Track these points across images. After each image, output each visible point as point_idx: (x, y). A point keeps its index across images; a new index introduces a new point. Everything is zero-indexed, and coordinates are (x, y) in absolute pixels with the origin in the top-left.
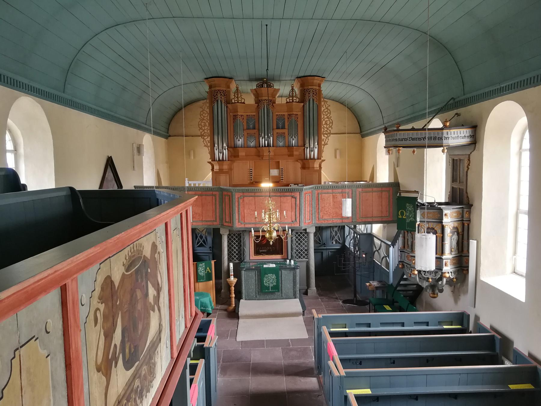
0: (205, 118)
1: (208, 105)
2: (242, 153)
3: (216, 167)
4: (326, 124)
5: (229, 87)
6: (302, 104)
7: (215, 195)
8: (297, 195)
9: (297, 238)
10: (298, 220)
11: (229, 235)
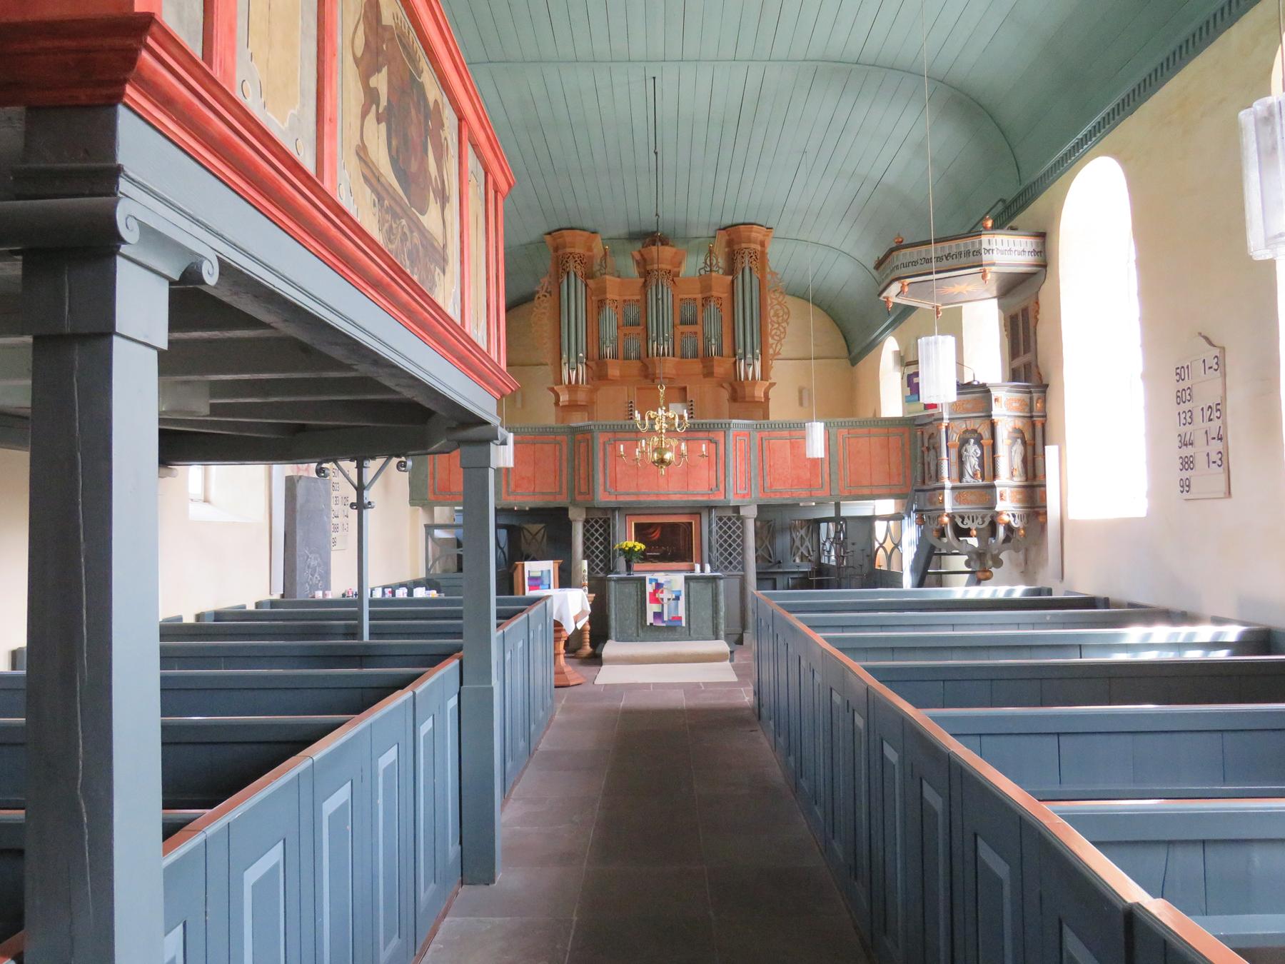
2: (614, 371)
3: (564, 398)
4: (776, 315)
5: (590, 249)
8: (720, 436)
9: (721, 528)
10: (721, 487)
11: (587, 521)
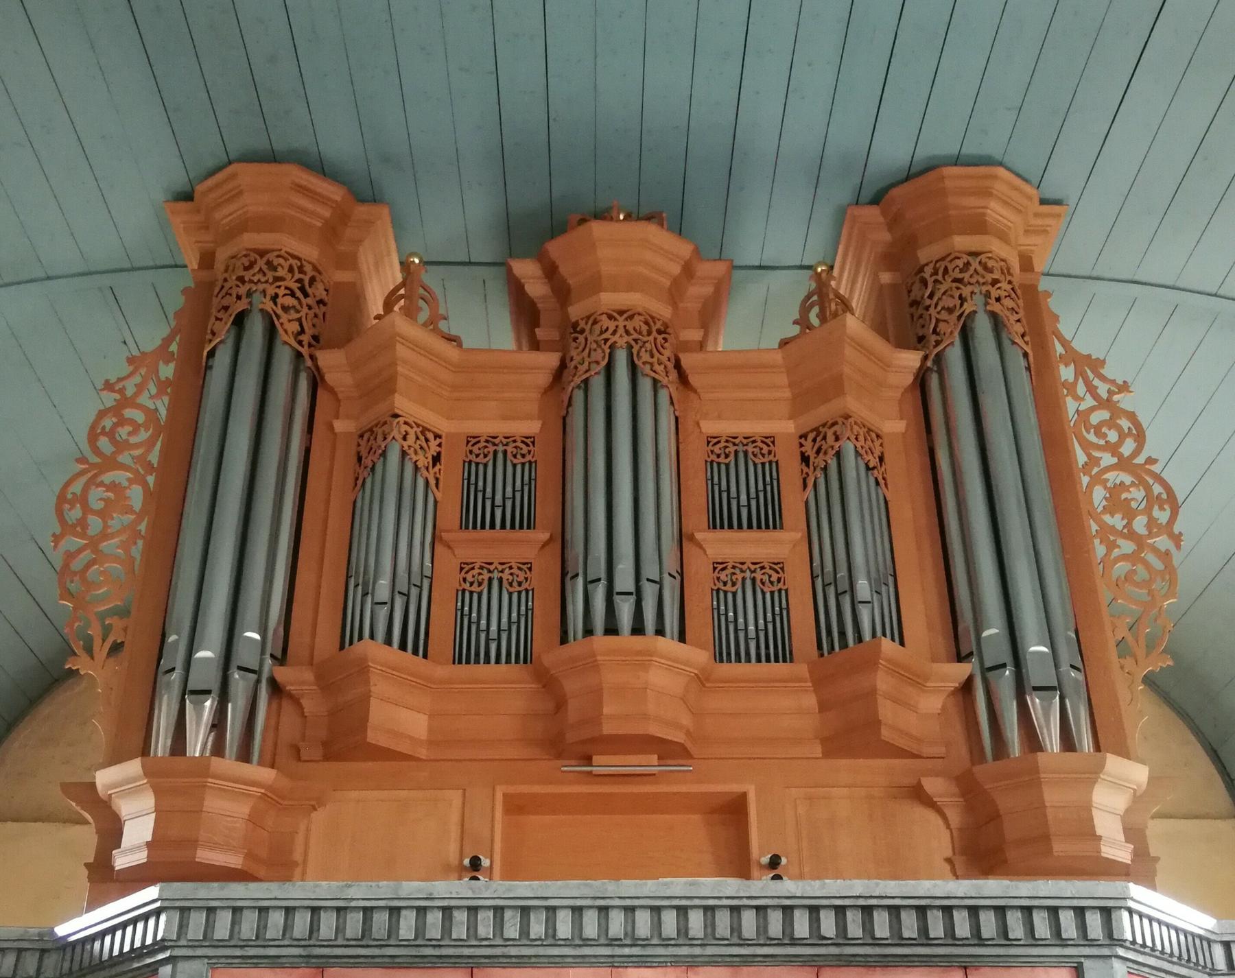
1: (167, 371)
4: (1116, 502)
5: (349, 261)
6: (911, 360)
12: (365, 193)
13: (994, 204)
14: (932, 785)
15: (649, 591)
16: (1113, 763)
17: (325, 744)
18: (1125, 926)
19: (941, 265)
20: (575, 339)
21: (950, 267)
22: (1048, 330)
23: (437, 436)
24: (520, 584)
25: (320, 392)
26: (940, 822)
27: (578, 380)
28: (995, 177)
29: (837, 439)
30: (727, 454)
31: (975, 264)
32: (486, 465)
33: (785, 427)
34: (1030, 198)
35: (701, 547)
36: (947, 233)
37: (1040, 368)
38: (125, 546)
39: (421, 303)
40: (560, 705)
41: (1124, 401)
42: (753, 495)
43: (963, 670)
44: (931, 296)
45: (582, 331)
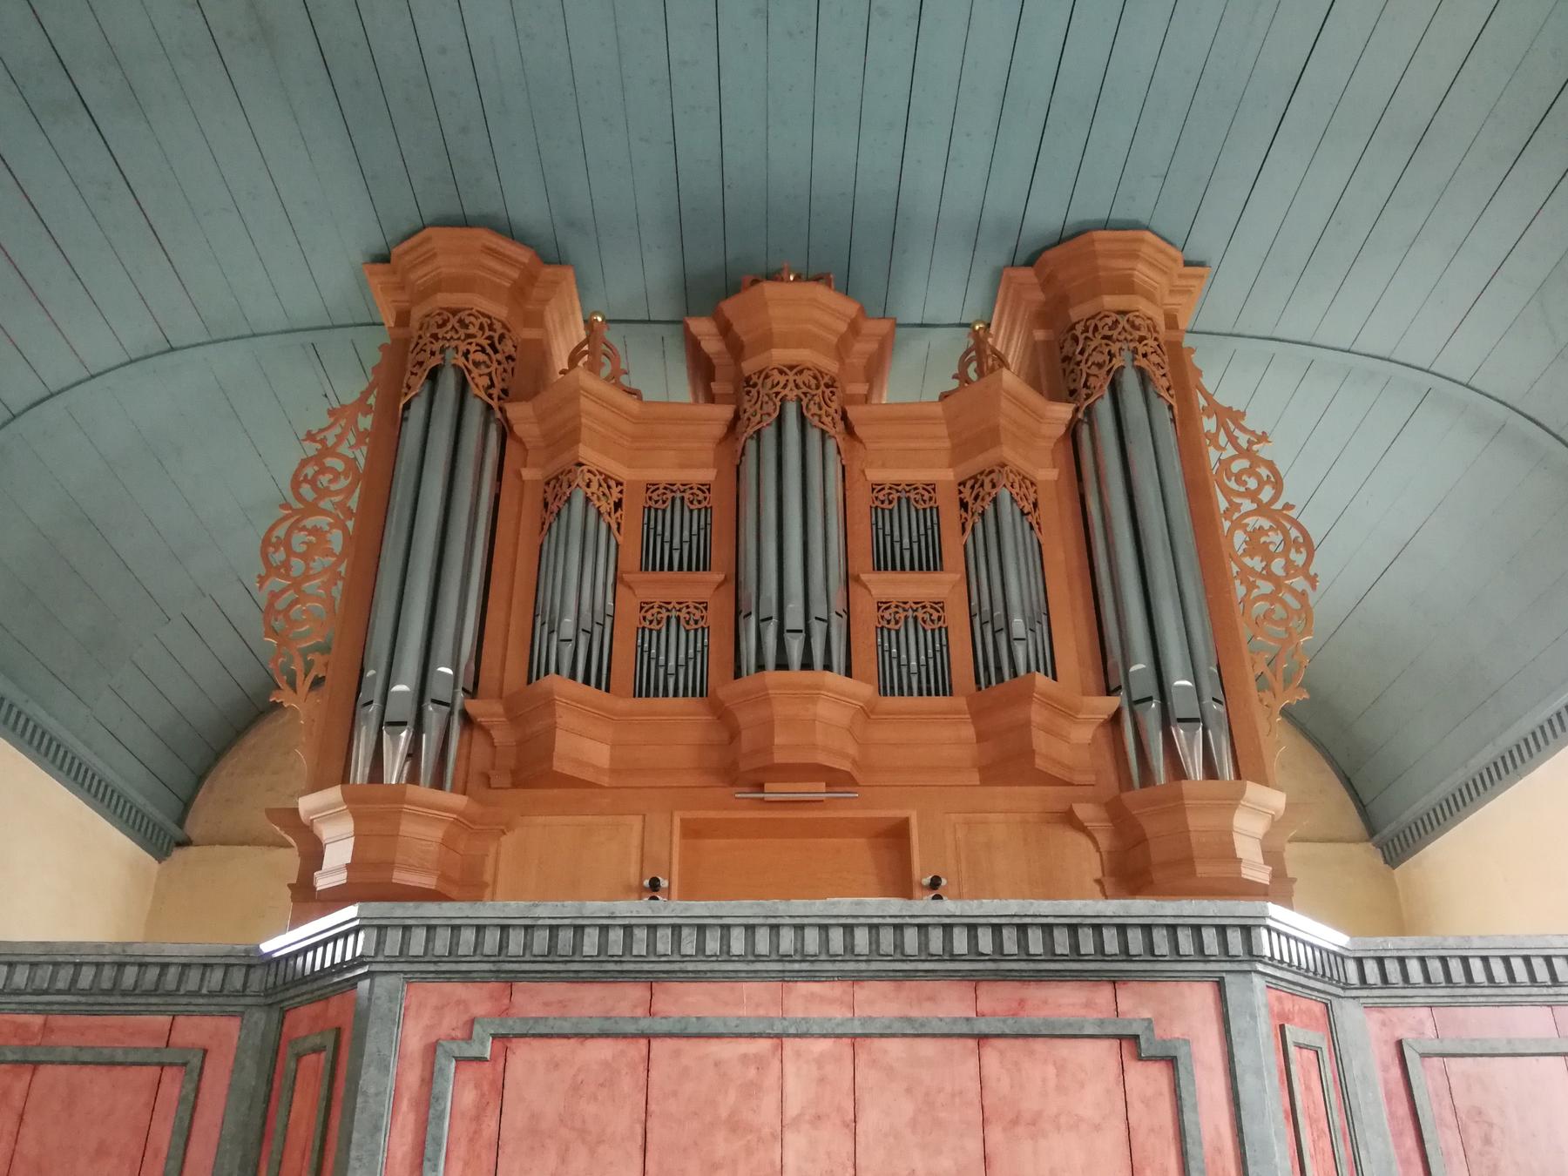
0: (326, 504)
1: (365, 422)
4: (1255, 545)
5: (536, 320)
6: (1063, 412)
7: (193, 1066)
8: (1188, 1014)
12: (551, 256)
13: (1141, 266)
14: (1083, 811)
15: (818, 629)
16: (1253, 790)
17: (514, 773)
18: (1265, 943)
19: (1092, 323)
20: (748, 393)
21: (1100, 325)
22: (1192, 383)
23: (619, 484)
24: (696, 622)
25: (509, 441)
26: (1091, 846)
27: (751, 431)
28: (1142, 241)
29: (994, 486)
30: (893, 501)
31: (1123, 322)
32: (664, 511)
33: (944, 475)
34: (1175, 260)
35: (866, 587)
36: (1096, 293)
37: (1184, 420)
38: (327, 586)
39: (604, 359)
40: (734, 735)
41: (1264, 451)
42: (915, 538)
43: (1113, 703)
44: (1082, 353)
45: (755, 385)
